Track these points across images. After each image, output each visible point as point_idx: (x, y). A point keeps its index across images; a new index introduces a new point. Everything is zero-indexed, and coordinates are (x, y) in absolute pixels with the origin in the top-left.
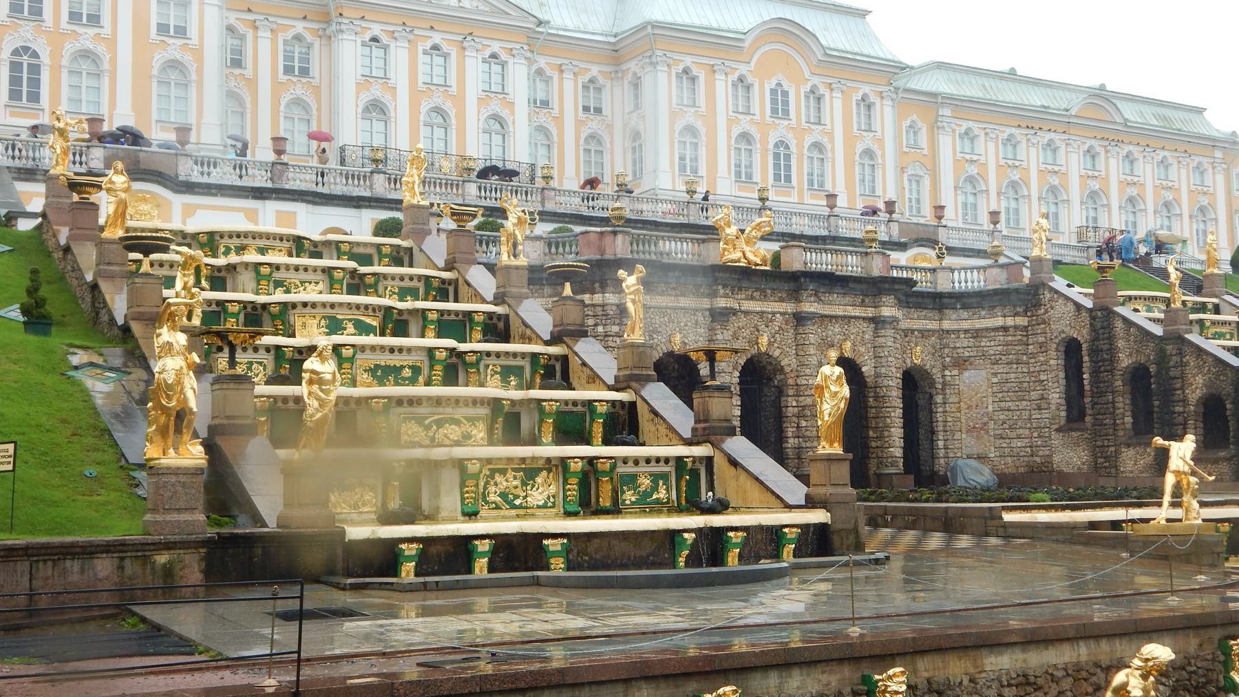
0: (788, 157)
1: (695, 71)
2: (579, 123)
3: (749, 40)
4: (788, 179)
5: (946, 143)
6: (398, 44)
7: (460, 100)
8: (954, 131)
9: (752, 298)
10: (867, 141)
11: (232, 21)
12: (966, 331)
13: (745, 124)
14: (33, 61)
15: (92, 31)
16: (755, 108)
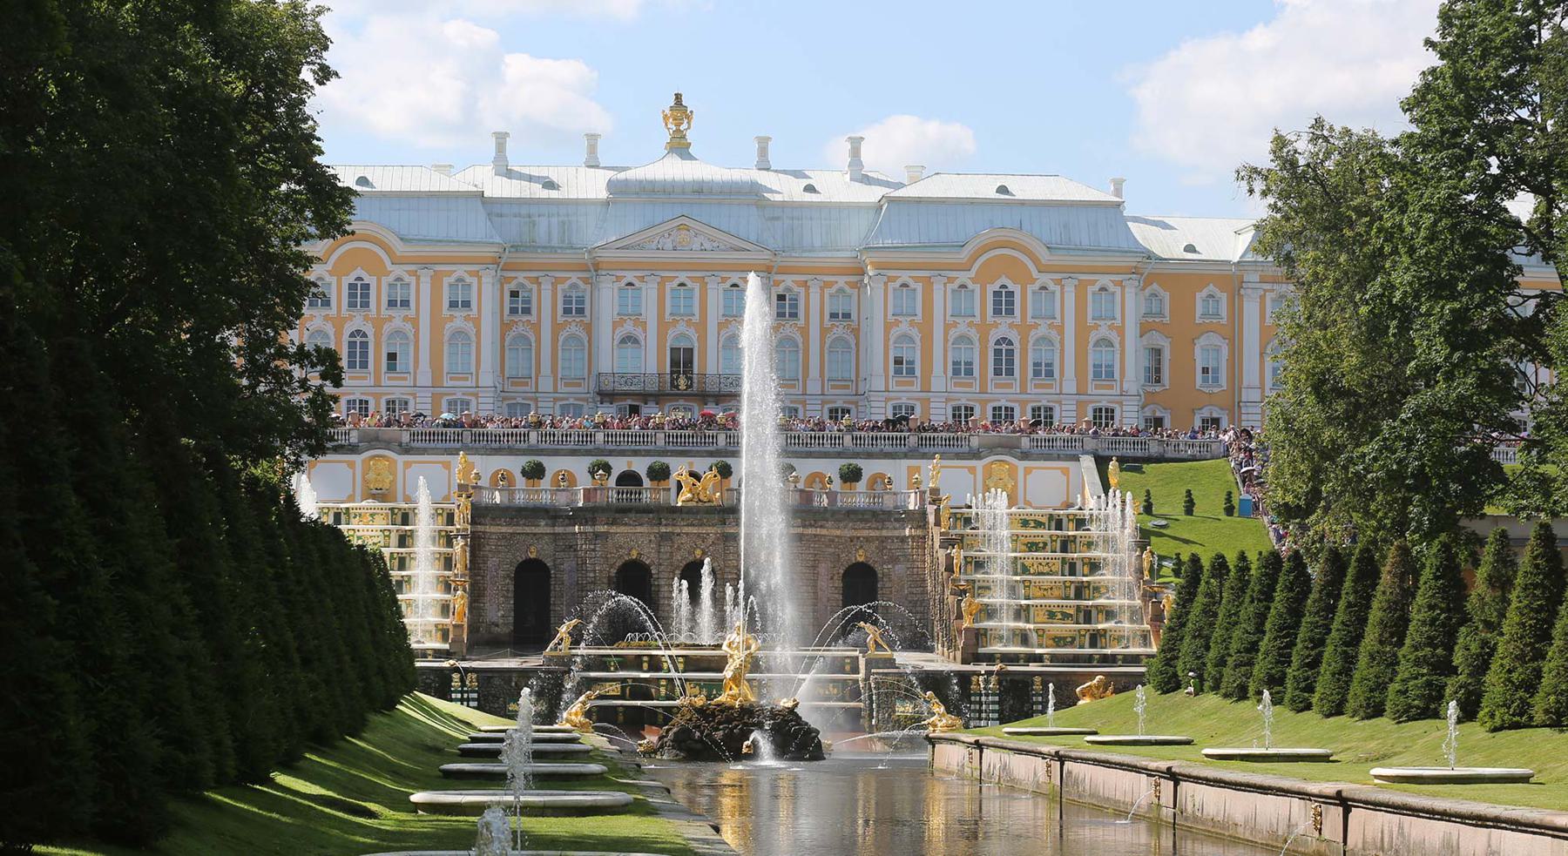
0: (1010, 353)
1: (912, 285)
2: (824, 332)
3: (964, 255)
4: (1010, 372)
5: (1251, 310)
6: (650, 286)
7: (702, 326)
8: (1262, 298)
9: (692, 525)
10: (1104, 331)
11: (521, 280)
12: (897, 538)
13: (962, 328)
14: (364, 339)
15: (404, 312)
16: (977, 312)
